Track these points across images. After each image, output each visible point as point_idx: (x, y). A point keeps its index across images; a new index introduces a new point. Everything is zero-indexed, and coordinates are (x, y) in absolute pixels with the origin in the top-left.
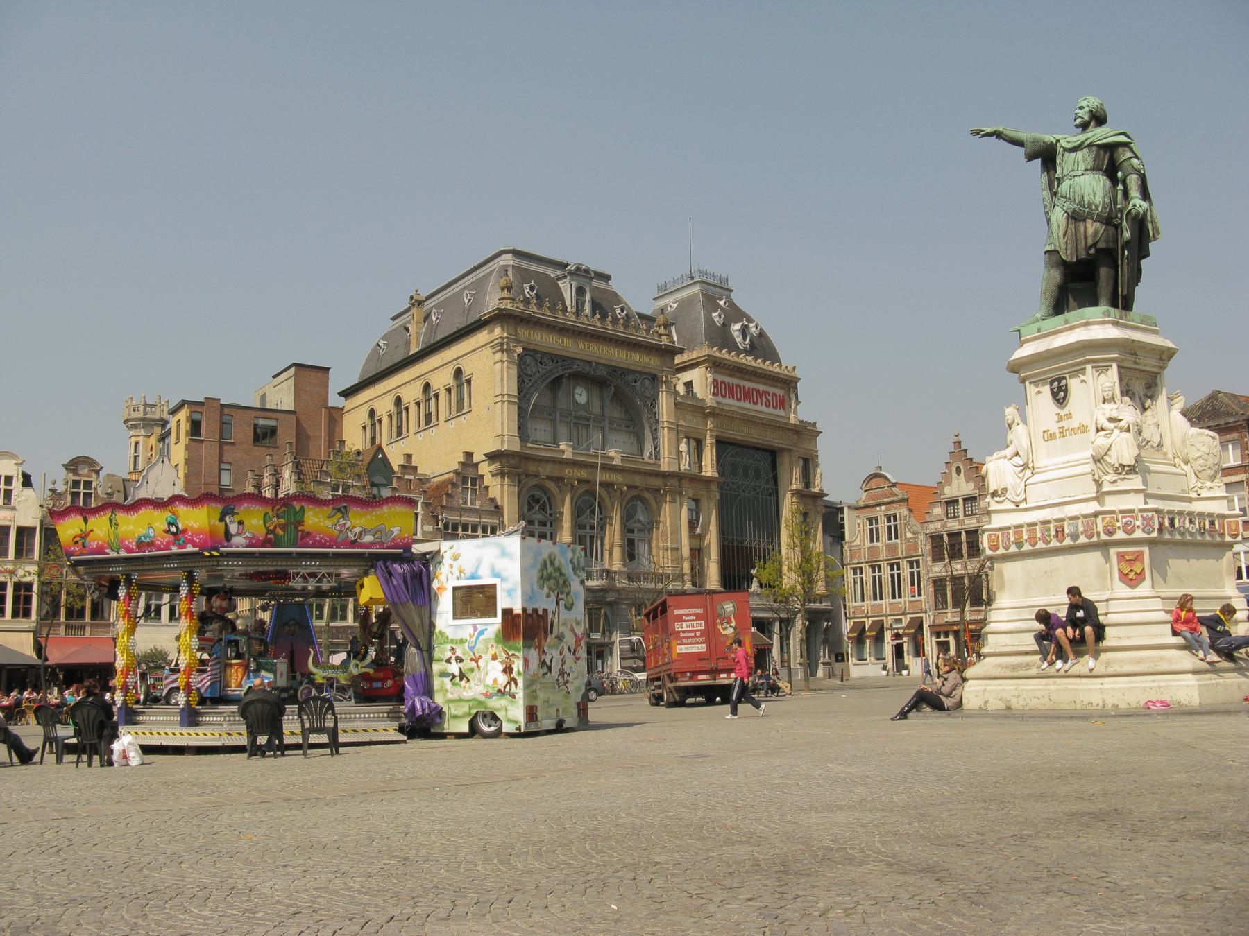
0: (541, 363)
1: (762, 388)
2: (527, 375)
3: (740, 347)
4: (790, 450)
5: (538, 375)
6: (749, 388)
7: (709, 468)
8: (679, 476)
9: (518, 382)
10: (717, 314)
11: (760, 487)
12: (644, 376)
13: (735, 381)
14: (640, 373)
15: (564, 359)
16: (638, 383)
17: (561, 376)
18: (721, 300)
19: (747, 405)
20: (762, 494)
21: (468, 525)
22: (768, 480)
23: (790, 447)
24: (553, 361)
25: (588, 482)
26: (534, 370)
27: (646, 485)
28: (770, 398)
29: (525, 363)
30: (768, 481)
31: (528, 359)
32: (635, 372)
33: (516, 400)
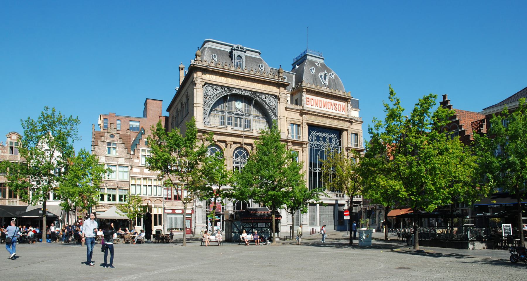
0: (216, 89)
4: (347, 130)
5: (214, 95)
6: (326, 102)
7: (305, 137)
10: (312, 68)
11: (331, 146)
12: (270, 96)
14: (269, 94)
15: (228, 88)
16: (267, 99)
18: (317, 62)
20: (333, 149)
22: (336, 144)
23: (347, 128)
24: (222, 89)
25: (240, 143)
28: (337, 106)
31: (209, 88)
32: (265, 94)
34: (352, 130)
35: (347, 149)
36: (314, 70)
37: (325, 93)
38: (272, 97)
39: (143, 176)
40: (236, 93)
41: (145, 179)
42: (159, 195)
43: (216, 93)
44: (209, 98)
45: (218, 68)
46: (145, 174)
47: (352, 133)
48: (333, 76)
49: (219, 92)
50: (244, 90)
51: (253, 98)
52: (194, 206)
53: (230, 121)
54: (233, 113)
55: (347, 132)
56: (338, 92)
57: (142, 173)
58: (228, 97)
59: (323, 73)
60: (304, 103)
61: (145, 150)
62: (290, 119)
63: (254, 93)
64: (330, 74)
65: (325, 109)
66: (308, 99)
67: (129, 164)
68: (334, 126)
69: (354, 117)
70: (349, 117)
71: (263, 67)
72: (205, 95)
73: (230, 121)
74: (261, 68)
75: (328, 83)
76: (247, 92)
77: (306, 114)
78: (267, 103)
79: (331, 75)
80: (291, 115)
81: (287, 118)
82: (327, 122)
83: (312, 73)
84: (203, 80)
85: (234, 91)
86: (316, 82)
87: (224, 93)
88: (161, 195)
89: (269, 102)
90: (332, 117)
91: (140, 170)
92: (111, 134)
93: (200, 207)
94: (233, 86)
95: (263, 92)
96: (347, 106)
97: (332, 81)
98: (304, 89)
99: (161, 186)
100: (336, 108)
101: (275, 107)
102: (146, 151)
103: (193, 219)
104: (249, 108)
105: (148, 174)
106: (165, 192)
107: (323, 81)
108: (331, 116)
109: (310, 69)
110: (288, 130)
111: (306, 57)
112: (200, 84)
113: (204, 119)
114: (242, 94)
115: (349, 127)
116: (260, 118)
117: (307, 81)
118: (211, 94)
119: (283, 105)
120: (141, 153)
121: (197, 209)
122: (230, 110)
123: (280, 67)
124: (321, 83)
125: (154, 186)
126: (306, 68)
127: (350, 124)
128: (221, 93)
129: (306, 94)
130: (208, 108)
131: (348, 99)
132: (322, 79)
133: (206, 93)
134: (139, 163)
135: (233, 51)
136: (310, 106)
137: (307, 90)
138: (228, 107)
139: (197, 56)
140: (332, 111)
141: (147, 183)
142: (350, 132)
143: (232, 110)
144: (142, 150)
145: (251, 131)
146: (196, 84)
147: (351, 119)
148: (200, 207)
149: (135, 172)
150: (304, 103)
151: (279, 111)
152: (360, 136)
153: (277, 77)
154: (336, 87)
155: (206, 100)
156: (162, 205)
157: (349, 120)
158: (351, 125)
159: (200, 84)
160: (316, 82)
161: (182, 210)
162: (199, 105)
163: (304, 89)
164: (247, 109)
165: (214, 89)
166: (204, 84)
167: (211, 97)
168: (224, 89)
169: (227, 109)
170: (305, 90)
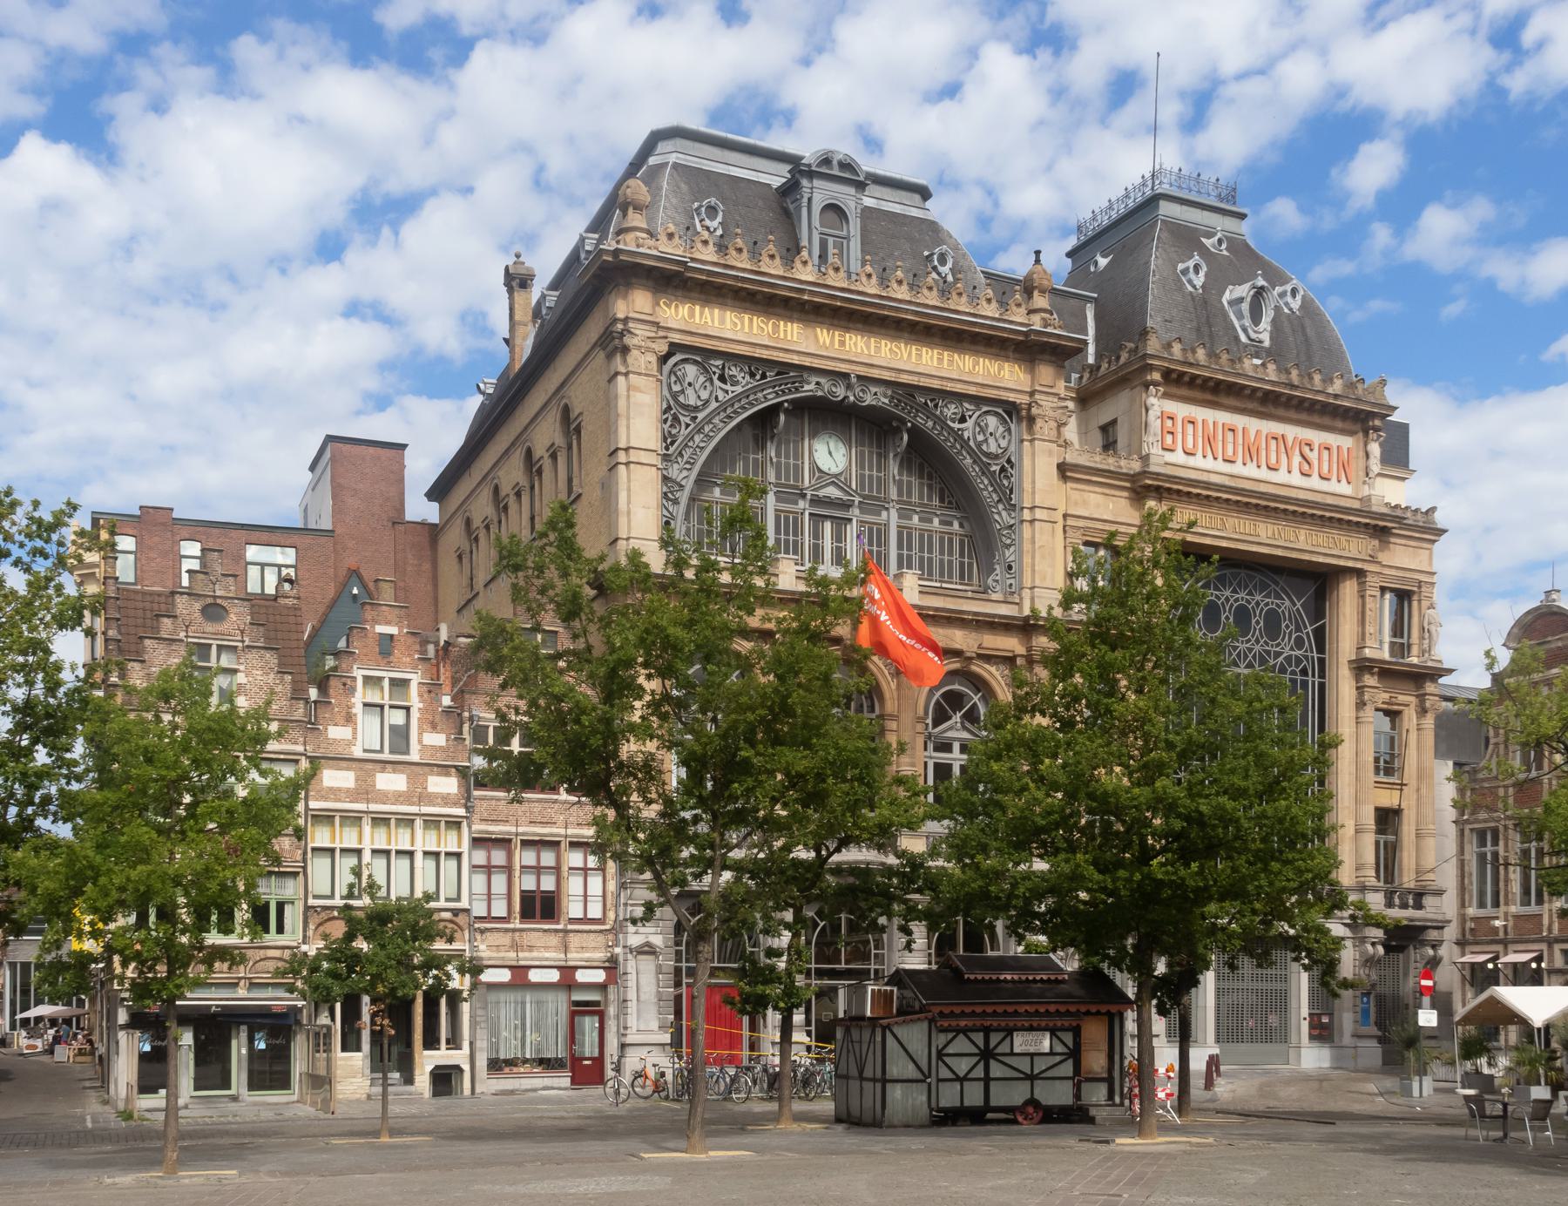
0: (722, 379)
1: (1292, 432)
2: (686, 407)
3: (1243, 338)
4: (1360, 574)
5: (714, 405)
9: (665, 421)
10: (1191, 263)
12: (985, 409)
13: (1224, 417)
14: (977, 400)
15: (783, 368)
16: (970, 423)
17: (773, 410)
23: (1359, 565)
24: (752, 375)
26: (705, 395)
27: (980, 647)
28: (1313, 456)
30: (1299, 643)
31: (691, 371)
32: (960, 397)
33: (654, 459)
34: (1387, 571)
35: (1362, 667)
36: (1202, 274)
37: (1255, 390)
38: (997, 414)
39: (373, 807)
40: (820, 393)
41: (380, 821)
42: (447, 900)
43: (721, 395)
44: (687, 420)
46: (384, 797)
47: (1383, 589)
48: (1296, 304)
49: (739, 389)
50: (859, 377)
51: (903, 421)
52: (618, 950)
53: (787, 533)
54: (803, 496)
55: (1362, 584)
56: (1324, 381)
57: (364, 791)
58: (782, 417)
59: (1247, 286)
60: (1151, 439)
61: (380, 679)
62: (1081, 523)
63: (906, 392)
64: (1278, 289)
65: (1251, 470)
66: (1169, 423)
67: (300, 748)
68: (1294, 555)
69: (1397, 506)
70: (1374, 509)
71: (949, 265)
72: (669, 408)
73: (787, 533)
74: (941, 269)
75: (1271, 339)
76: (874, 390)
77: (1159, 492)
78: (972, 443)
79: (1283, 295)
80: (1085, 503)
81: (1065, 516)
82: (1263, 534)
83: (1190, 288)
84: (661, 334)
85: (809, 388)
86: (1211, 336)
87: (760, 395)
88: (458, 899)
89: (980, 438)
91: (357, 780)
92: (210, 601)
93: (648, 950)
94: (807, 362)
95: (949, 386)
96: (1362, 454)
97: (1288, 330)
98: (1151, 368)
99: (458, 855)
100: (1306, 467)
101: (1009, 461)
102: (386, 683)
103: (612, 1010)
104: (879, 470)
105: (398, 797)
106: (480, 880)
107: (1245, 330)
108: (1282, 506)
109: (1181, 266)
111: (1157, 207)
112: (649, 350)
113: (667, 523)
114: (852, 398)
115: (1373, 560)
116: (931, 521)
117: (1168, 330)
118: (699, 403)
119: (1050, 453)
120: (361, 695)
121: (631, 966)
122: (788, 479)
123: (1037, 261)
124: (1237, 338)
125: (426, 853)
126: (1160, 261)
127: (1376, 542)
128: (745, 393)
129: (1166, 395)
130: (685, 473)
131: (1372, 415)
132: (1240, 316)
133: (675, 396)
134: (351, 743)
136: (1178, 457)
137: (1167, 374)
138: (779, 463)
140: (1288, 478)
141: (389, 843)
142: (1373, 582)
143: (796, 480)
144: (367, 679)
146: (625, 350)
147: (1382, 516)
148: (648, 950)
149: (331, 789)
150: (1151, 439)
151: (1027, 485)
152: (1425, 604)
153: (1023, 310)
154: (1309, 358)
156: (467, 947)
157: (1373, 522)
158: (1381, 550)
159: (649, 350)
160: (1211, 336)
163: (1151, 368)
164: (871, 477)
165: (715, 378)
166: (663, 348)
167: (701, 416)
168: (764, 376)
169: (771, 476)
170: (1156, 376)
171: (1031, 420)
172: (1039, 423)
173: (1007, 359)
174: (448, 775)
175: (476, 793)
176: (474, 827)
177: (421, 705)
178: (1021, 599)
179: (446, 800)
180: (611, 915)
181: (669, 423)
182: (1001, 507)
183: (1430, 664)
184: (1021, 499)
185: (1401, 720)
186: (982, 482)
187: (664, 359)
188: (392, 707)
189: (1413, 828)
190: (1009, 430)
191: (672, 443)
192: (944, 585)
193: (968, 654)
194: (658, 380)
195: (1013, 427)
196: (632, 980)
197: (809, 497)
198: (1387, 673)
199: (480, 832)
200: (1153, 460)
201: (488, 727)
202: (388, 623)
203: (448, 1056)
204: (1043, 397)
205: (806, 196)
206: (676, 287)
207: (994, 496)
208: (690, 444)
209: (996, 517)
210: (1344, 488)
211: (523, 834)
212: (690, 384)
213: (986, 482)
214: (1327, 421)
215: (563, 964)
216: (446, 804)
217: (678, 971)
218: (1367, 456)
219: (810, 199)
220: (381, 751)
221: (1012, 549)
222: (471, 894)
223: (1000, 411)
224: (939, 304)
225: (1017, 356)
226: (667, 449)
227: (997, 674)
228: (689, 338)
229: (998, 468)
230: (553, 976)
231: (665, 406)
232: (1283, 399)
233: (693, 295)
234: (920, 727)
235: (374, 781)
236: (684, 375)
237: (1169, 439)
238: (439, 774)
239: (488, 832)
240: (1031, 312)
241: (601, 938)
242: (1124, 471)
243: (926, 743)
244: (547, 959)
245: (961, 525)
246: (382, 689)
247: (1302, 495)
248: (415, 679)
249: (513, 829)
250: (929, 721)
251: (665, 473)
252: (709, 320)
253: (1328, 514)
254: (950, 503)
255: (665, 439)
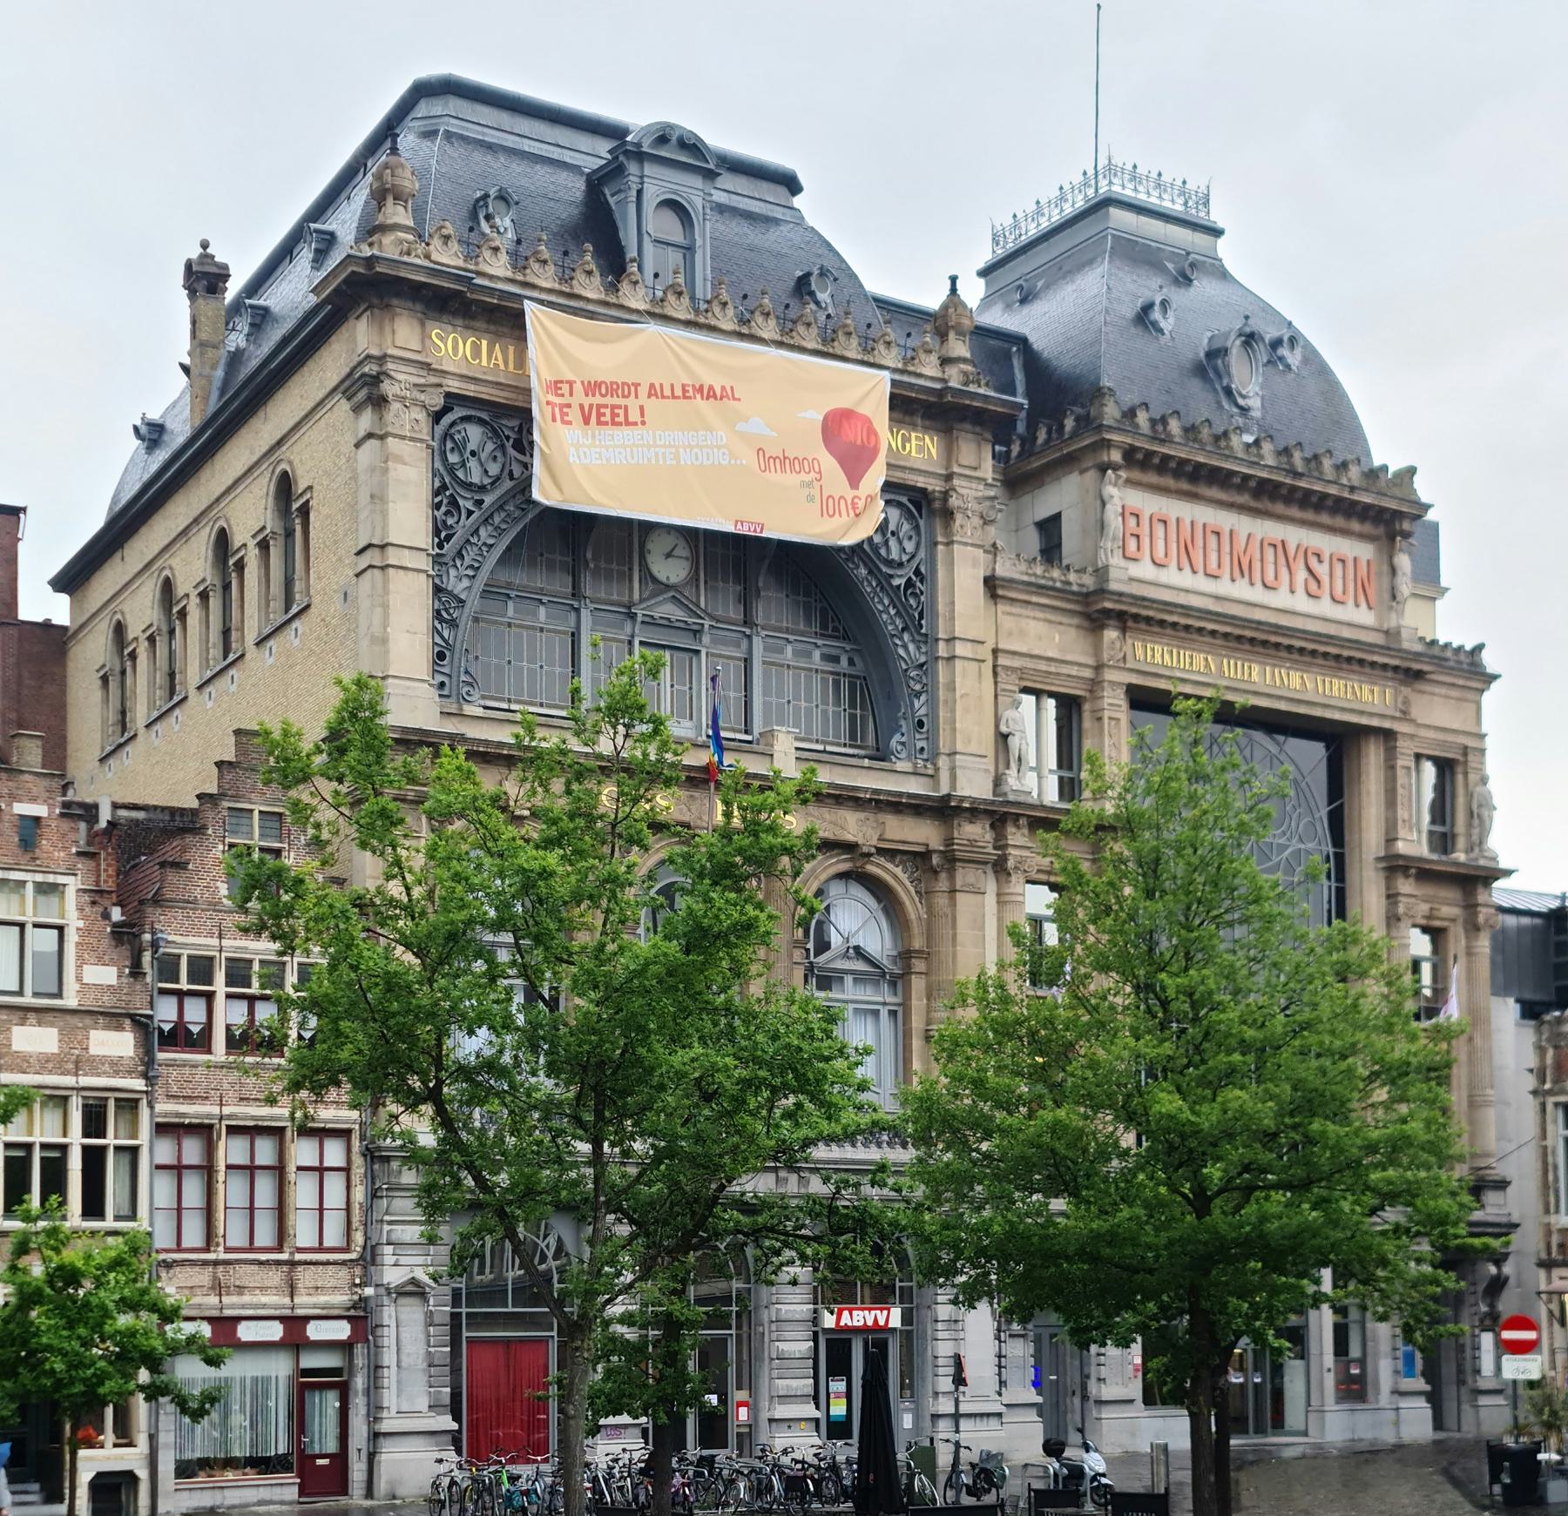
1: (1295, 536)
2: (468, 486)
4: (1388, 736)
8: (1000, 815)
9: (437, 506)
19: (1241, 590)
21: (250, 961)
23: (1387, 724)
27: (880, 839)
28: (1322, 570)
29: (459, 447)
31: (474, 433)
33: (424, 563)
34: (1423, 733)
35: (1395, 866)
37: (1246, 477)
44: (470, 505)
45: (533, 286)
47: (1418, 757)
62: (1017, 663)
65: (1241, 590)
68: (1302, 710)
70: (1406, 645)
72: (444, 487)
80: (1022, 634)
81: (995, 652)
90: (1298, 644)
96: (1385, 568)
98: (1108, 444)
99: (134, 1151)
100: (1313, 586)
101: (917, 572)
102: (30, 887)
105: (46, 1063)
110: (1003, 738)
112: (415, 403)
115: (1405, 716)
118: (487, 481)
119: (975, 564)
129: (1130, 482)
133: (451, 470)
135: (632, 168)
136: (1144, 570)
137: (1130, 454)
139: (390, 200)
141: (30, 1134)
142: (1406, 749)
145: (760, 748)
147: (1417, 656)
152: (1472, 777)
153: (934, 359)
155: (450, 521)
161: (281, 1319)
162: (408, 559)
163: (1108, 444)
165: (509, 445)
166: (437, 401)
167: (489, 499)
170: (1116, 456)
171: (948, 515)
172: (959, 518)
173: (914, 426)
174: (120, 1028)
175: (161, 1056)
176: (159, 1108)
177: (81, 924)
178: (937, 769)
179: (116, 1066)
180: (359, 1238)
181: (443, 509)
182: (906, 636)
183: (1482, 862)
184: (934, 626)
185: (1446, 941)
186: (881, 602)
187: (437, 417)
188: (36, 926)
189: (1464, 1094)
190: (917, 528)
191: (448, 538)
192: (829, 748)
193: (865, 850)
194: (428, 447)
195: (922, 523)
196: (388, 1337)
197: (640, 618)
198: (1426, 874)
199: (166, 1115)
200: (1113, 573)
201: (179, 956)
202: (33, 800)
203: (116, 1458)
204: (964, 483)
205: (635, 187)
206: (454, 314)
207: (898, 621)
208: (474, 540)
209: (901, 652)
210: (1365, 617)
211: (230, 1117)
212: (473, 453)
213: (886, 602)
214: (1339, 521)
215: (287, 1312)
216: (116, 1073)
217: (455, 1317)
218: (1393, 571)
219: (640, 192)
220: (20, 993)
221: (923, 698)
222: (152, 1209)
223: (904, 500)
224: (820, 347)
225: (927, 423)
226: (440, 546)
227: (904, 877)
228: (472, 387)
229: (903, 581)
230: (275, 1331)
231: (437, 484)
232: (1284, 491)
233: (477, 324)
234: (798, 955)
235: (9, 1039)
236: (466, 440)
237: (1132, 544)
238: (107, 1028)
239: (178, 1115)
240: (945, 361)
241: (343, 1273)
242: (1075, 588)
243: (806, 977)
244: (264, 1306)
245: (851, 662)
246: (23, 897)
247: (1312, 626)
248: (73, 884)
249: (216, 1110)
250: (810, 946)
251: (437, 581)
252: (501, 362)
253: (1346, 653)
254: (835, 629)
255: (437, 532)
